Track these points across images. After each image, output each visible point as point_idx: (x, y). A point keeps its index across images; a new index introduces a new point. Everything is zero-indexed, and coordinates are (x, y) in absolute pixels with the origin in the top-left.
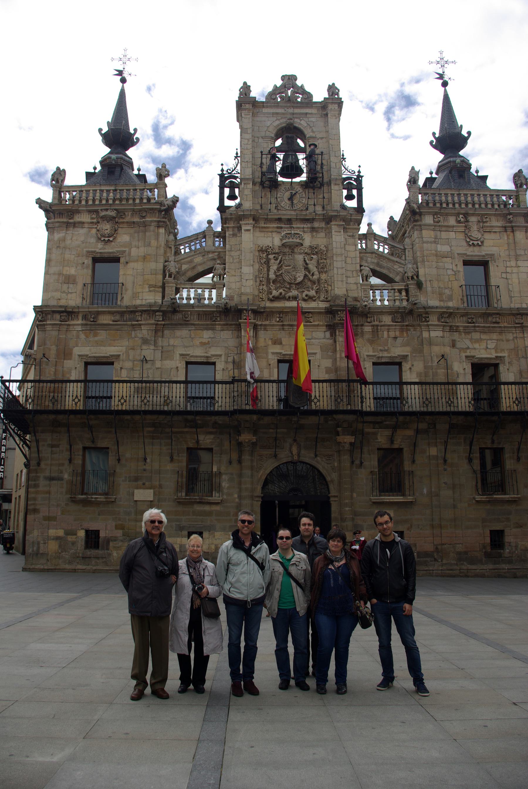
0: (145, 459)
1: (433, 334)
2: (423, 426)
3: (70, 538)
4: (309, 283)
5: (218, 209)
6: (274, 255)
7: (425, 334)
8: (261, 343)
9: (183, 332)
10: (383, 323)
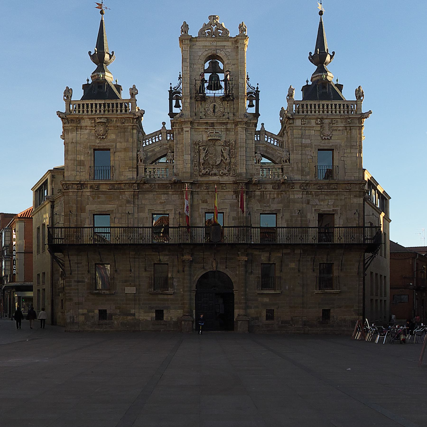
0: (131, 270)
2: (288, 251)
3: (91, 314)
4: (224, 164)
5: (169, 114)
6: (203, 147)
8: (195, 203)
9: (150, 196)
10: (267, 190)
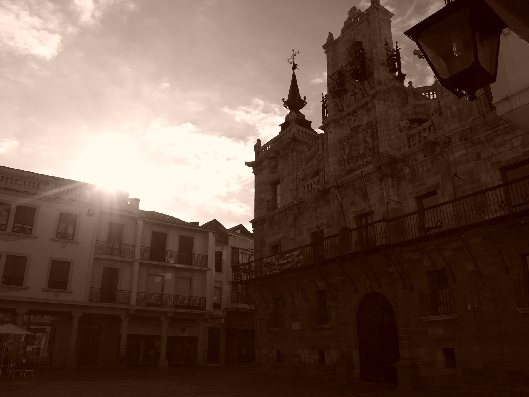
1: (457, 155)
7: (451, 158)
